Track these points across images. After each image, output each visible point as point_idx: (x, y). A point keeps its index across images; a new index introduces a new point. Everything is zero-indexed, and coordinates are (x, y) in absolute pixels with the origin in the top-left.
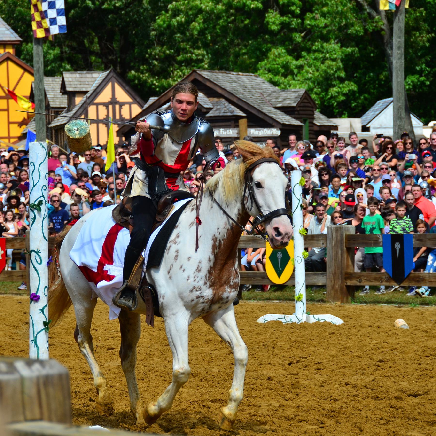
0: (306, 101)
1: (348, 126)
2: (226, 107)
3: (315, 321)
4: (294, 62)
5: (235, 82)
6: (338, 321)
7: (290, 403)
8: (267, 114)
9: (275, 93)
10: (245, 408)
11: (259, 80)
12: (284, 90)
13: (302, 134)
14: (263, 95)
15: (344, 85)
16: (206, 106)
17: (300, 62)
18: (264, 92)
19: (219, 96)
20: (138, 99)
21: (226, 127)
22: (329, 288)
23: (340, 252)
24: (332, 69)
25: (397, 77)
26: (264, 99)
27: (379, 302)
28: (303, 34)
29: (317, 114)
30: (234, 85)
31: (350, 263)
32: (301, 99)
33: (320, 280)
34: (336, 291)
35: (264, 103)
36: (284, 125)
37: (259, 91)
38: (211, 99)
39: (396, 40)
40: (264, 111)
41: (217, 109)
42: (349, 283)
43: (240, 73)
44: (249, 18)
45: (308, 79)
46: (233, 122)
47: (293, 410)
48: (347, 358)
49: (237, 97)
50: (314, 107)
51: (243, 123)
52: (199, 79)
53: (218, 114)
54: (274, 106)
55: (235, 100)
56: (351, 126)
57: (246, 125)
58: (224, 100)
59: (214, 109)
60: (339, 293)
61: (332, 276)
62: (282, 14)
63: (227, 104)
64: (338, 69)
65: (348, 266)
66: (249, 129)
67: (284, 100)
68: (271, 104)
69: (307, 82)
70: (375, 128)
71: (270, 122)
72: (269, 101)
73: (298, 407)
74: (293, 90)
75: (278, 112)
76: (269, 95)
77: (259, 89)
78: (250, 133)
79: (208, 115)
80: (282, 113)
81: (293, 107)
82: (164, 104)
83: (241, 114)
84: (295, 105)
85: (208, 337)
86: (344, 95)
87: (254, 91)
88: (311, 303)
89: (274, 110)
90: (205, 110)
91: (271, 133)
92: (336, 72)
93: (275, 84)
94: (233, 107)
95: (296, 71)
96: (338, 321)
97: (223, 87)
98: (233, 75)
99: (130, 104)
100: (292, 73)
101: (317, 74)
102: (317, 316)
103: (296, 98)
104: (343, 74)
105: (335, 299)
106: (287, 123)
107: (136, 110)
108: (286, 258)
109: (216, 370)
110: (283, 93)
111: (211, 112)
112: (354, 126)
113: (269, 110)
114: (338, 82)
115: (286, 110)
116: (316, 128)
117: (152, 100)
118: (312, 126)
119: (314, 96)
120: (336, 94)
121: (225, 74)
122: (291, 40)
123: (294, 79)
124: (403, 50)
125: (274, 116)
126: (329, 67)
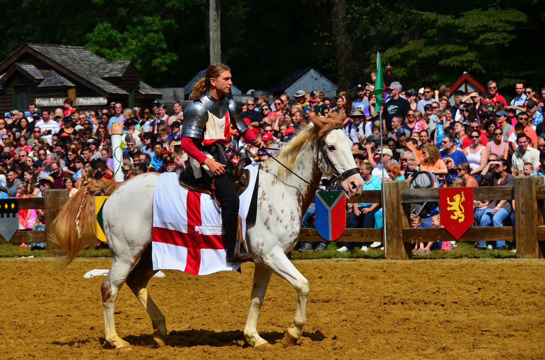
0: (131, 71)
1: (172, 94)
2: (56, 78)
4: (119, 35)
5: (65, 54)
8: (95, 84)
9: (102, 65)
11: (87, 53)
12: (110, 61)
13: (128, 103)
14: (91, 67)
15: (166, 56)
16: (37, 78)
17: (126, 35)
18: (92, 64)
19: (50, 68)
21: (56, 97)
24: (155, 41)
25: (214, 48)
26: (92, 71)
28: (127, 10)
29: (142, 84)
30: (64, 57)
32: (126, 69)
37: (87, 63)
38: (42, 71)
39: (213, 14)
40: (92, 82)
41: (48, 81)
43: (69, 47)
45: (132, 50)
49: (66, 69)
52: (31, 52)
53: (49, 85)
54: (102, 77)
55: (65, 72)
56: (175, 95)
57: (74, 94)
58: (54, 72)
59: (46, 80)
64: (161, 41)
66: (77, 99)
67: (111, 70)
68: (99, 75)
69: (131, 53)
71: (98, 91)
72: (96, 72)
74: (119, 61)
75: (106, 82)
76: (97, 66)
77: (87, 61)
78: (79, 103)
79: (39, 86)
80: (109, 83)
81: (119, 77)
83: (71, 84)
84: (121, 75)
86: (166, 65)
87: (82, 63)
89: (101, 81)
90: (36, 82)
91: (99, 102)
92: (158, 43)
94: (62, 78)
95: (121, 44)
97: (53, 59)
98: (63, 48)
100: (117, 45)
101: (139, 44)
103: (122, 69)
104: (165, 46)
106: (114, 92)
110: (110, 64)
111: (42, 83)
112: (178, 95)
113: (96, 80)
114: (160, 53)
115: (113, 80)
118: (138, 95)
119: (138, 66)
120: (159, 65)
121: (54, 48)
123: (120, 51)
124: (219, 23)
126: (151, 39)
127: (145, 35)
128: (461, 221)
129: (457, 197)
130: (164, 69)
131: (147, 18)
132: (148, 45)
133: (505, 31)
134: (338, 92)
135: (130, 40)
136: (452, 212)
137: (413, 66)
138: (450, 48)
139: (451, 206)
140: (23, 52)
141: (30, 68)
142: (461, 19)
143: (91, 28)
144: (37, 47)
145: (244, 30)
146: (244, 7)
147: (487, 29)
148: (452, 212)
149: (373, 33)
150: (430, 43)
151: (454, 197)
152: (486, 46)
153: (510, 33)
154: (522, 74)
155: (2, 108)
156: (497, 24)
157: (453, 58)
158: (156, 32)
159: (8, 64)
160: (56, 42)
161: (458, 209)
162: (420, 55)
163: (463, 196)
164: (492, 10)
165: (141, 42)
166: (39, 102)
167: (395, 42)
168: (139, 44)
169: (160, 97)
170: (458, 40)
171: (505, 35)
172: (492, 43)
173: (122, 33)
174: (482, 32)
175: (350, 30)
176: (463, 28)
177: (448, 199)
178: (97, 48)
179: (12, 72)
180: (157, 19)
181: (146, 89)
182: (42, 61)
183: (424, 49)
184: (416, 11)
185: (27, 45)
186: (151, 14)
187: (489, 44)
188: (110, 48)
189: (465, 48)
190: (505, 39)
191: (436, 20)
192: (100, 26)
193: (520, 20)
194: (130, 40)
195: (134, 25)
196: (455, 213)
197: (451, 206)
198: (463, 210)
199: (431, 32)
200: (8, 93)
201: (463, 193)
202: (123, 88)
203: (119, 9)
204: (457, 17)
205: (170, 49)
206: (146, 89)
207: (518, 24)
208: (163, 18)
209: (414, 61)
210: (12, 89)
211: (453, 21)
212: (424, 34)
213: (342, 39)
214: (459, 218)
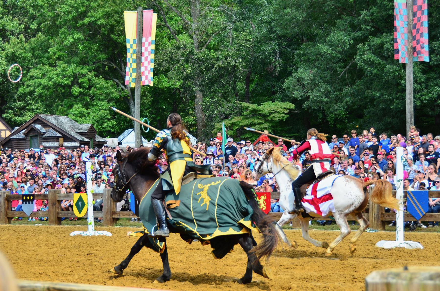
1: (111, 142)
3: (98, 234)
4: (86, 111)
6: (109, 234)
7: (89, 273)
10: (67, 275)
11: (69, 119)
12: (81, 124)
17: (89, 111)
20: (9, 128)
22: (104, 219)
23: (109, 202)
27: (128, 226)
29: (97, 136)
30: (57, 121)
31: (114, 207)
33: (100, 215)
34: (108, 221)
35: (71, 130)
36: (81, 141)
42: (114, 216)
44: (64, 89)
46: (56, 139)
47: (90, 276)
48: (115, 252)
50: (96, 132)
51: (61, 140)
52: (40, 118)
55: (57, 129)
57: (63, 141)
60: (109, 222)
61: (106, 213)
62: (80, 87)
63: (53, 131)
64: (107, 114)
65: (113, 208)
70: (124, 143)
71: (74, 139)
73: (93, 275)
75: (78, 135)
82: (22, 130)
83: (60, 135)
84: (86, 131)
85: (46, 243)
88: (96, 226)
93: (77, 121)
95: (87, 115)
96: (109, 234)
98: (56, 117)
99: (5, 130)
100: (85, 116)
101: (96, 116)
102: (99, 232)
104: (109, 117)
105: (107, 224)
107: (8, 133)
108: (83, 205)
109: (51, 258)
113: (74, 134)
115: (82, 134)
116: (96, 143)
117: (16, 129)
119: (95, 127)
122: (84, 100)
125: (76, 137)
126: (103, 113)
127: (99, 111)
130: (109, 129)
131: (101, 103)
132: (101, 116)
133: (284, 113)
134: (197, 142)
135: (91, 114)
137: (237, 130)
138: (256, 121)
140: (36, 118)
141: (39, 127)
142: (261, 106)
143: (71, 107)
144: (43, 116)
145: (150, 109)
146: (150, 97)
147: (275, 112)
149: (216, 112)
150: (246, 118)
152: (274, 120)
153: (286, 114)
154: (292, 135)
155: (24, 147)
156: (279, 109)
157: (257, 126)
158: (105, 110)
159: (28, 124)
160: (52, 113)
162: (240, 124)
164: (277, 102)
165: (97, 115)
166: (44, 144)
167: (226, 118)
168: (96, 116)
169: (106, 143)
170: (260, 117)
171: (283, 115)
172: (277, 119)
173: (87, 109)
174: (272, 113)
175: (203, 111)
176: (262, 111)
178: (74, 117)
179: (29, 129)
180: (106, 102)
181: (99, 139)
182: (45, 123)
183: (242, 121)
184: (238, 102)
185: (37, 115)
186: (102, 100)
187: (275, 119)
188: (81, 117)
189: (263, 121)
190: (283, 117)
191: (249, 107)
192: (76, 106)
193: (291, 107)
194: (91, 114)
195: (93, 106)
199: (245, 113)
200: (28, 139)
202: (87, 138)
203: (85, 97)
204: (259, 105)
205: (112, 119)
206: (99, 139)
207: (290, 110)
208: (109, 102)
209: (237, 127)
210: (30, 137)
211: (258, 107)
212: (243, 114)
213: (200, 115)
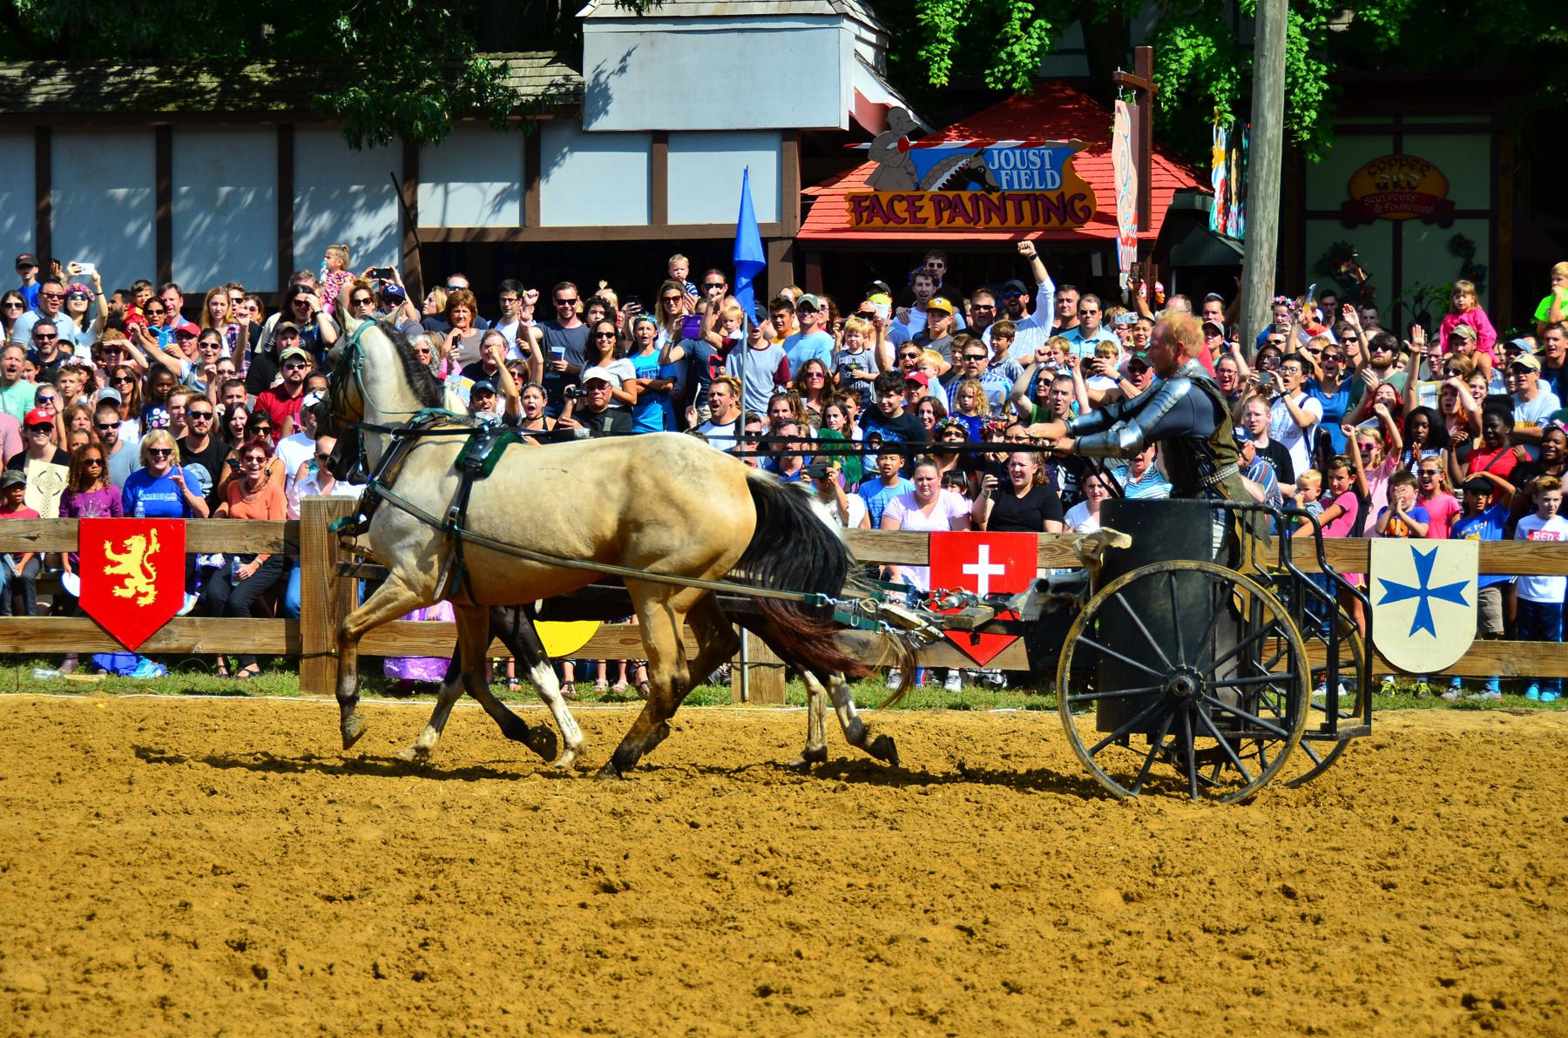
128: (142, 602)
129: (136, 543)
136: (120, 580)
139: (114, 564)
148: (120, 580)
151: (127, 542)
161: (137, 572)
163: (154, 540)
177: (108, 545)
196: (127, 582)
197: (114, 564)
198: (154, 574)
201: (154, 532)
214: (138, 594)
